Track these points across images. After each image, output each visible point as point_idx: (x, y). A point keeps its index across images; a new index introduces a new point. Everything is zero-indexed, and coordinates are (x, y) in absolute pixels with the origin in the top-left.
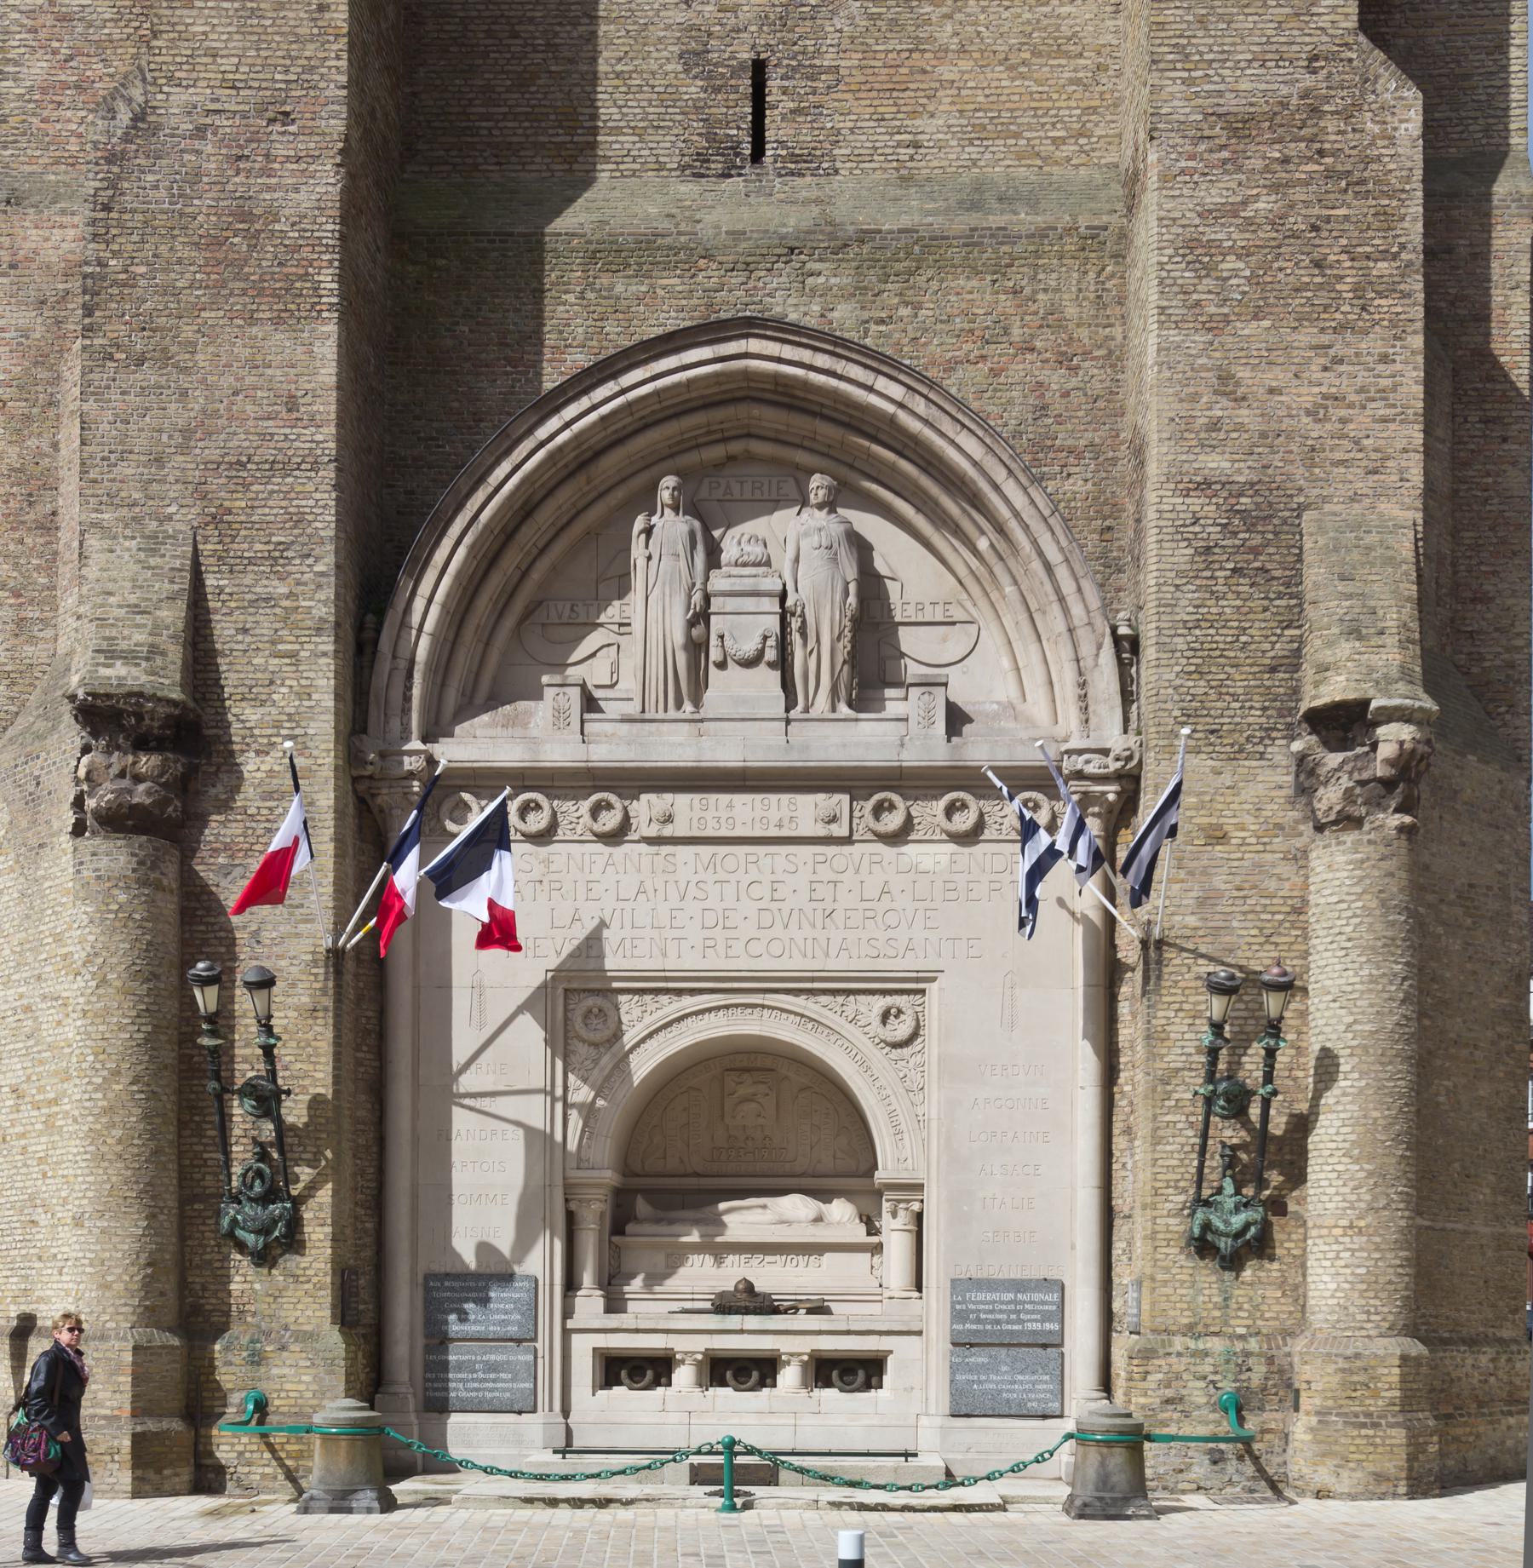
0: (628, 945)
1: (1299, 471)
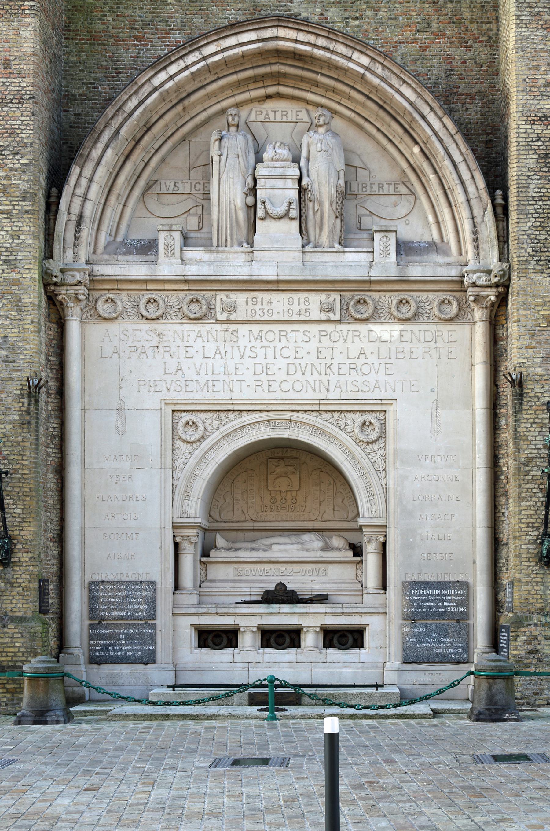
0: (210, 384)
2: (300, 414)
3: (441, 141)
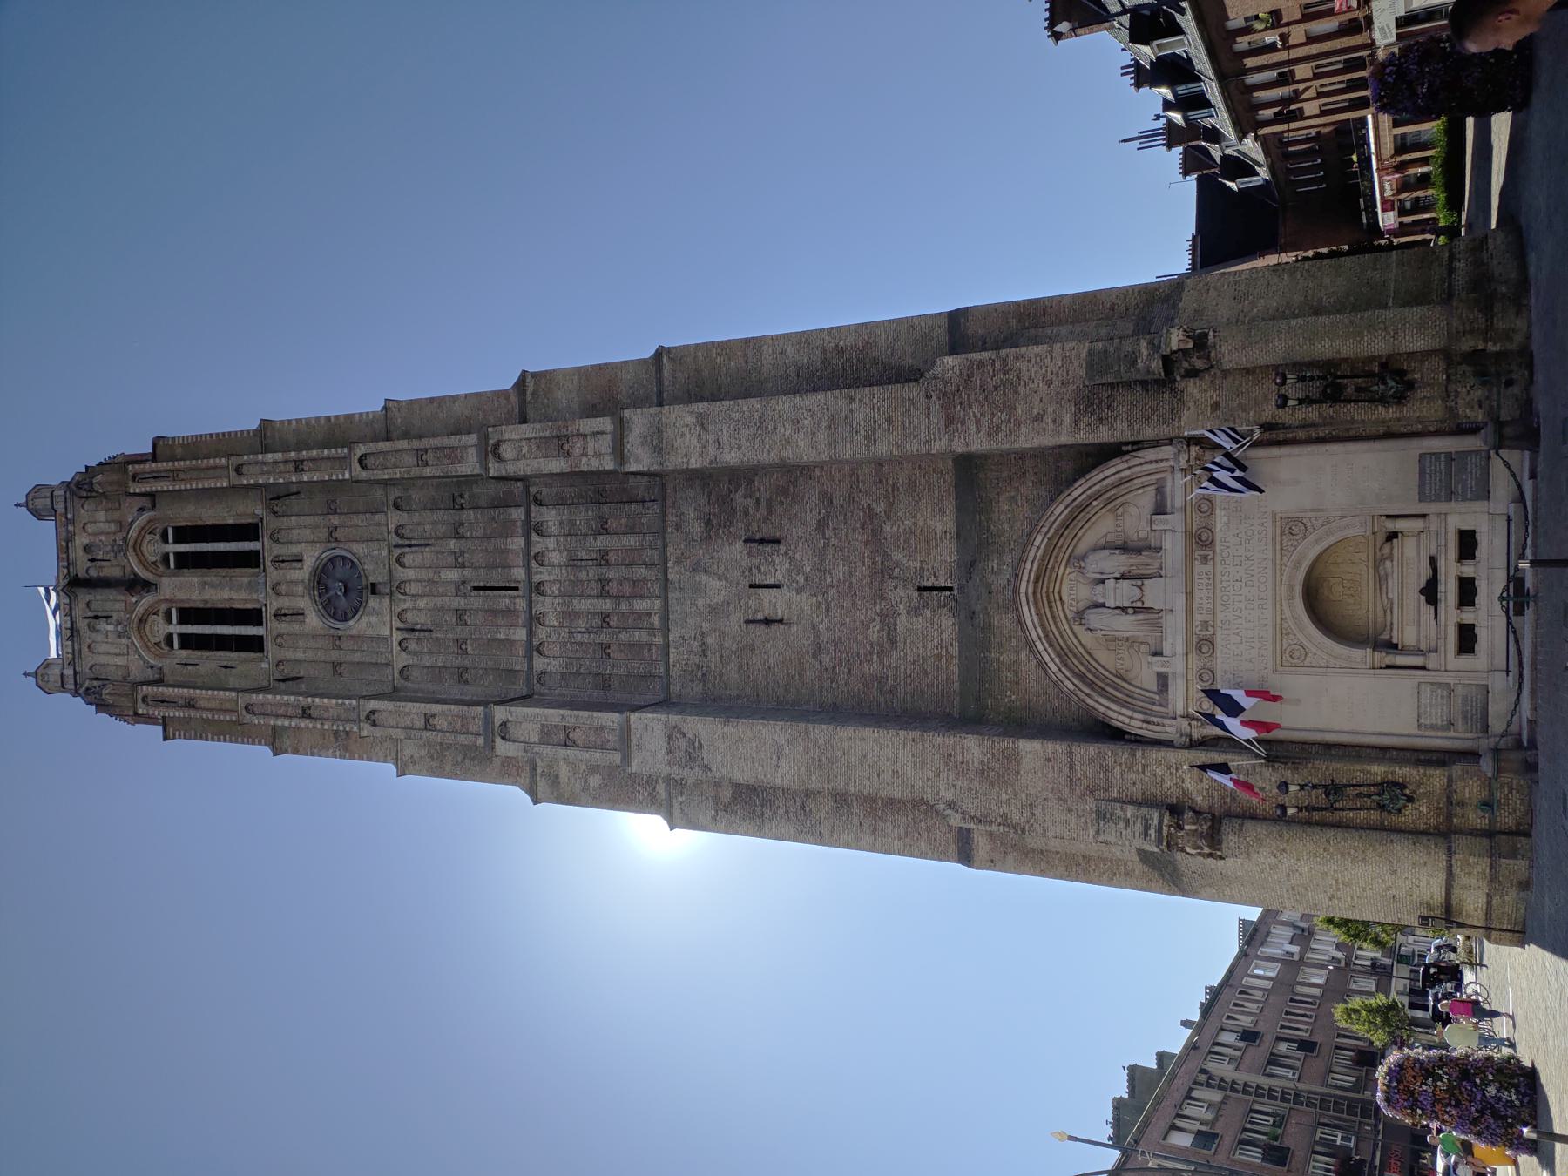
1: (1071, 387)
2: (1284, 578)
3: (1090, 488)
